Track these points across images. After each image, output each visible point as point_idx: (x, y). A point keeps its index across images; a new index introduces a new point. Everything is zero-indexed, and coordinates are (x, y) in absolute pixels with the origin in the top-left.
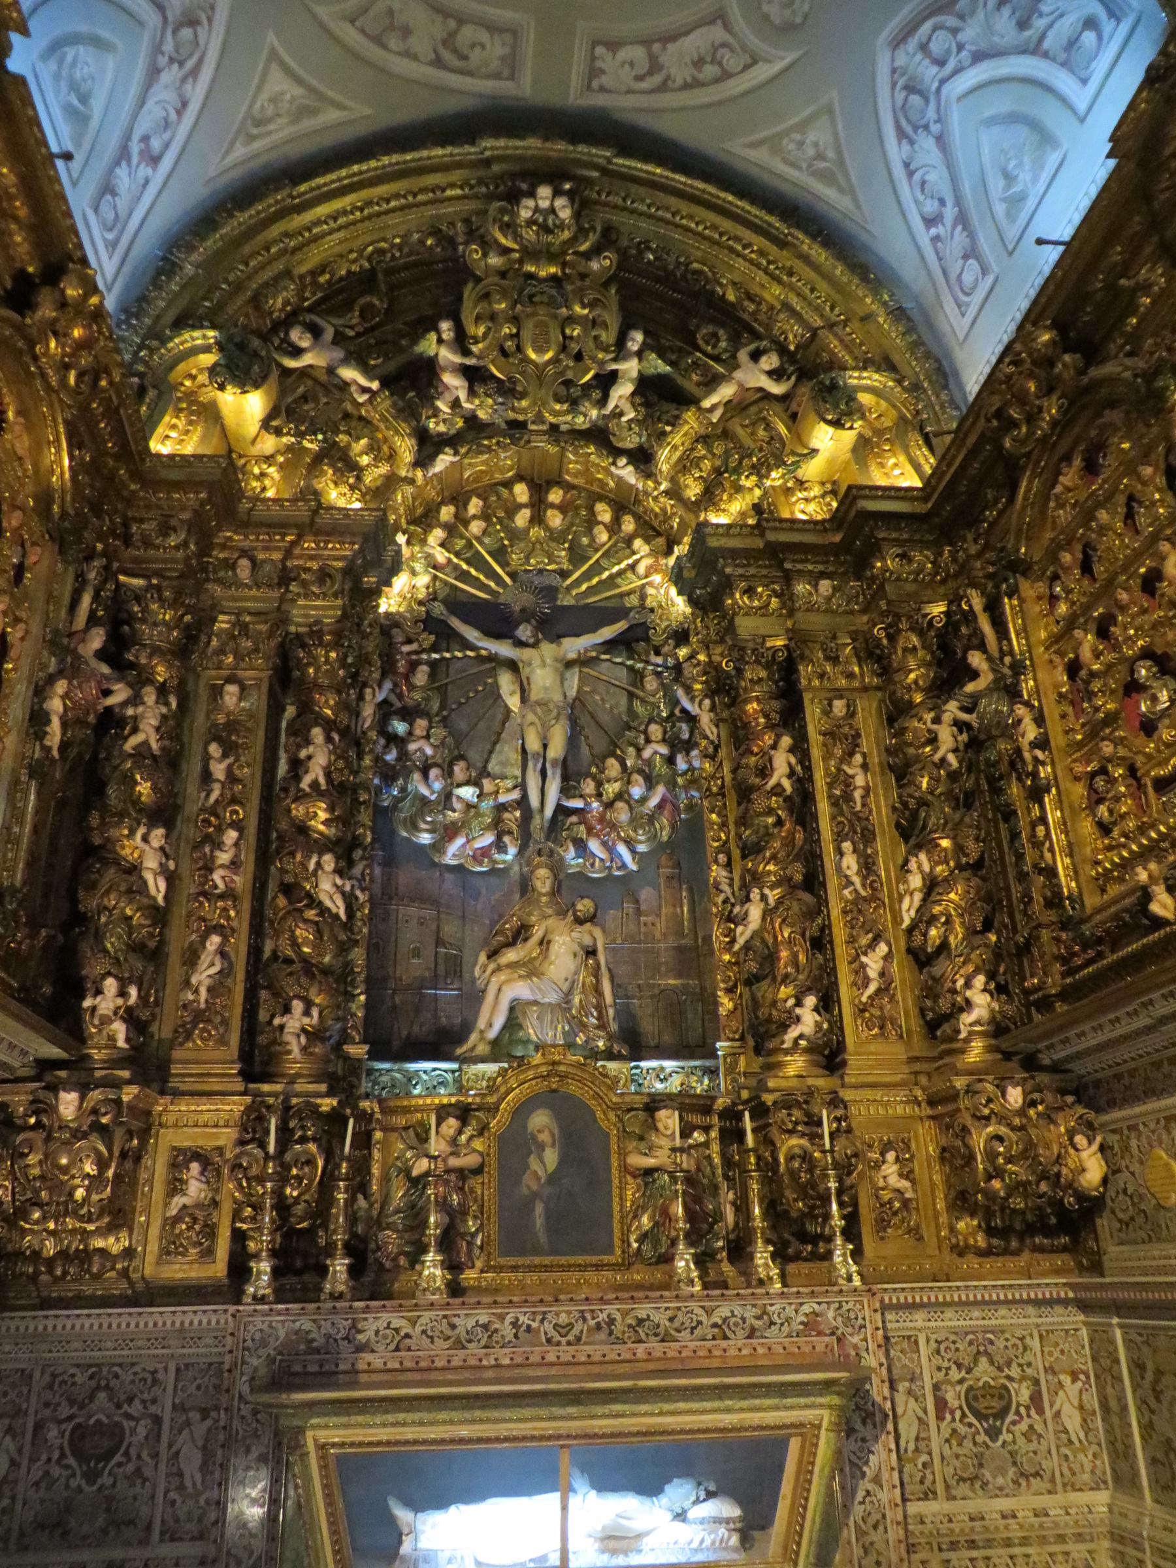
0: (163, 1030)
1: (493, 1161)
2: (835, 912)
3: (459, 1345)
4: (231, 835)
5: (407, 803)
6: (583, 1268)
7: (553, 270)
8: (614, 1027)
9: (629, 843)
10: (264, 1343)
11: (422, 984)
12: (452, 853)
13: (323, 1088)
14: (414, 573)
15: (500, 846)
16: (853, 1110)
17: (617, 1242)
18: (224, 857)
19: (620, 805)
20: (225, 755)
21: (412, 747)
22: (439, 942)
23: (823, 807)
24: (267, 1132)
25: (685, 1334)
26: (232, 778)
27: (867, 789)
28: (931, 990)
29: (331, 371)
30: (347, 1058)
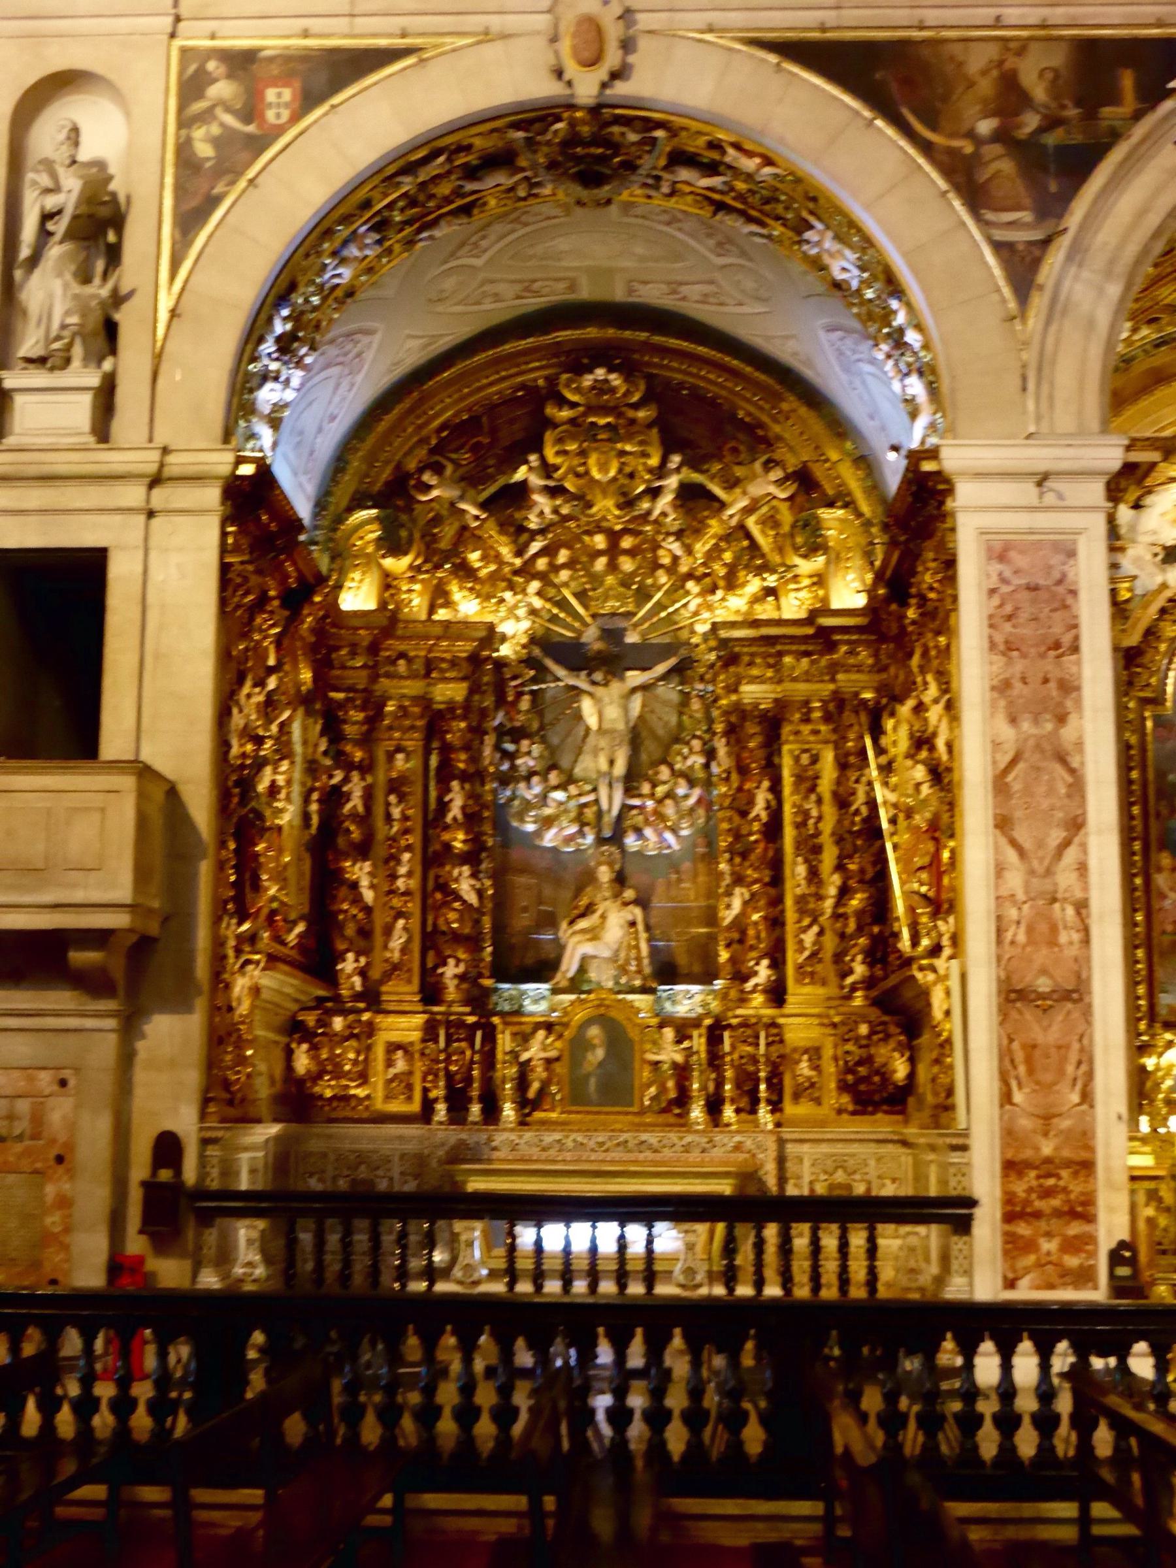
0: (375, 974)
2: (789, 902)
3: (544, 1149)
4: (406, 856)
5: (516, 803)
7: (609, 420)
9: (674, 830)
10: (443, 1144)
11: (528, 931)
12: (550, 839)
13: (467, 1009)
14: (518, 619)
15: (581, 833)
17: (636, 1101)
18: (403, 870)
19: (669, 802)
20: (400, 802)
21: (519, 762)
23: (789, 834)
24: (438, 1036)
25: (666, 1150)
26: (405, 818)
27: (820, 818)
29: (452, 504)
30: (481, 987)
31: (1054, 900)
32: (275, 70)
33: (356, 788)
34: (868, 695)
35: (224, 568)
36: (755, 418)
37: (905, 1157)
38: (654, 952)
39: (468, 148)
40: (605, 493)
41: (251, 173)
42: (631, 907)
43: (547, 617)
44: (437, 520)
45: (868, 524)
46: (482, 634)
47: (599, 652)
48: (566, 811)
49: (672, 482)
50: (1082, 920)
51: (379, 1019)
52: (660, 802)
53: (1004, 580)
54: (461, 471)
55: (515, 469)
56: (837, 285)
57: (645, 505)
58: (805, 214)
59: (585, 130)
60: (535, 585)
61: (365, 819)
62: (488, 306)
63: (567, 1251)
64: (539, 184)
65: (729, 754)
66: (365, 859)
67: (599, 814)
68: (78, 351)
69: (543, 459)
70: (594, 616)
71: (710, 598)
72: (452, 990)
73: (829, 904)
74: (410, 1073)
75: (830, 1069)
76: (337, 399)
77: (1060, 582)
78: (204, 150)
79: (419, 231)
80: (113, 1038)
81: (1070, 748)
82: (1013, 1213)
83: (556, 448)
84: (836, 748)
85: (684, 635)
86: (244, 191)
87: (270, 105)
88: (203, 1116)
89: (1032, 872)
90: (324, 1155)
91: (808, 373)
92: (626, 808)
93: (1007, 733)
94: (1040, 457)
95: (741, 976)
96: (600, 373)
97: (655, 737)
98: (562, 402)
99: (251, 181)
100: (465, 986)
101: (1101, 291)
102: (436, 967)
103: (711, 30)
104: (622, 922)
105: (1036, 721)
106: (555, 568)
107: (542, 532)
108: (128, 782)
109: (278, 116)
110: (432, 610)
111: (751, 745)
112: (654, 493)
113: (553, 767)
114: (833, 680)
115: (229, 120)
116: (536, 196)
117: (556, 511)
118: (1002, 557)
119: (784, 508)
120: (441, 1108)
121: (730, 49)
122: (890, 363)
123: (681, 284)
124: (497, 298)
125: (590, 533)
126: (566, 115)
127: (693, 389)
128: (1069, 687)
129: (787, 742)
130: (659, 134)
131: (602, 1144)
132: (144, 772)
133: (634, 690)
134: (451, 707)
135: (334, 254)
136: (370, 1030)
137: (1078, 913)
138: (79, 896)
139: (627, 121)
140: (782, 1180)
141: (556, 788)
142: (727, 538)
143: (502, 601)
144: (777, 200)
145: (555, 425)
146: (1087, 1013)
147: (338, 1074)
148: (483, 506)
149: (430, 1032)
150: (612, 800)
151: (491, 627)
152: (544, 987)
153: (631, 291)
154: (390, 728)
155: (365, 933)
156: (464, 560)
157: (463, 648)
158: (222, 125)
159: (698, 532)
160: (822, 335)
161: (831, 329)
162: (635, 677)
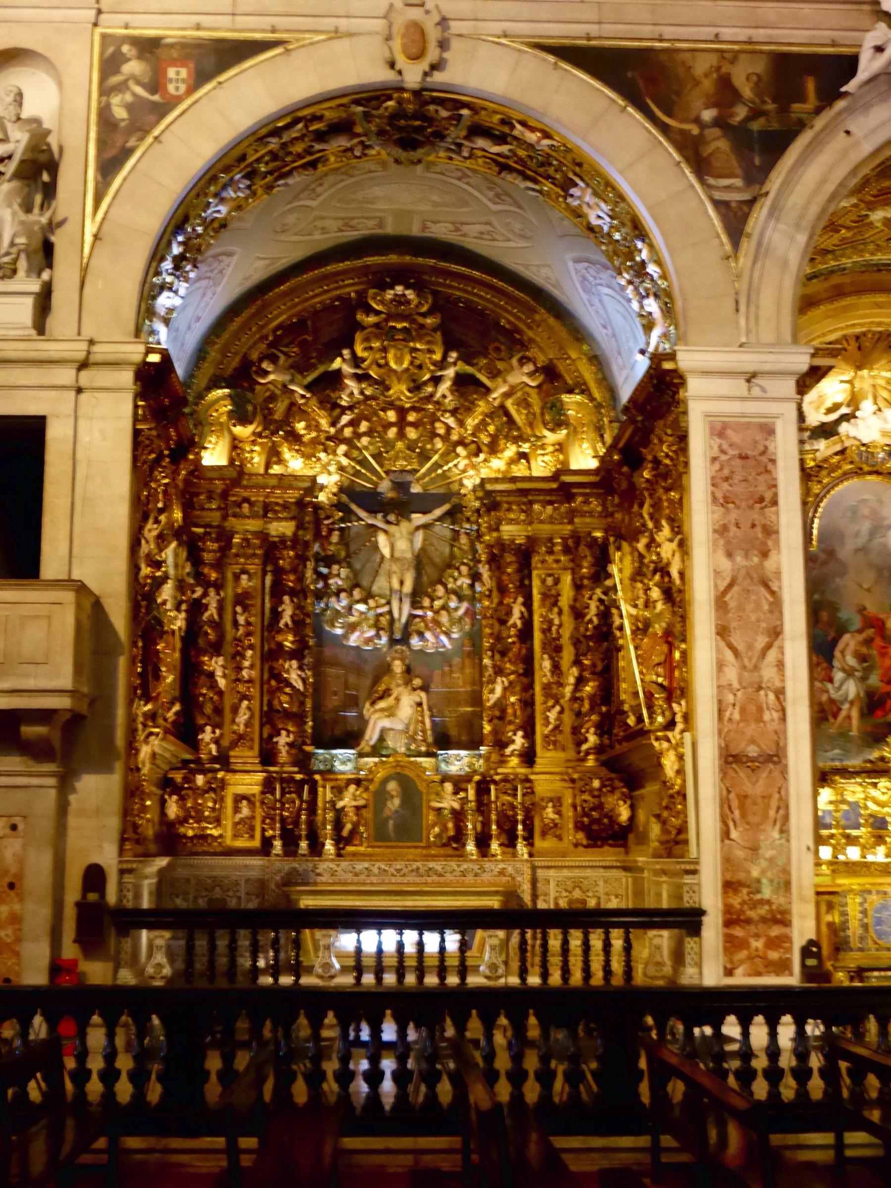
0: (225, 743)
1: (371, 803)
2: (538, 688)
3: (356, 875)
4: (249, 653)
6: (409, 847)
7: (405, 324)
8: (430, 739)
9: (447, 634)
10: (279, 871)
11: (337, 710)
12: (354, 640)
13: (296, 769)
14: (330, 473)
15: (378, 636)
16: (536, 784)
18: (246, 664)
21: (331, 581)
22: (347, 687)
23: (538, 636)
24: (275, 789)
26: (248, 624)
27: (560, 626)
28: (575, 730)
31: (760, 688)
32: (175, 54)
33: (212, 601)
34: (598, 534)
35: (136, 433)
36: (514, 325)
37: (625, 879)
38: (434, 724)
39: (320, 118)
40: (399, 380)
41: (156, 132)
42: (418, 692)
43: (351, 471)
44: (272, 398)
45: (599, 406)
46: (307, 484)
47: (392, 499)
48: (367, 619)
49: (450, 372)
50: (781, 703)
51: (229, 776)
52: (437, 612)
53: (723, 452)
54: (291, 361)
55: (332, 361)
56: (591, 229)
57: (430, 389)
58: (571, 175)
59: (410, 107)
60: (343, 448)
61: (218, 626)
62: (317, 236)
63: (380, 951)
64: (369, 147)
65: (491, 578)
66: (219, 655)
67: (392, 621)
68: (22, 264)
69: (353, 353)
70: (387, 472)
71: (474, 459)
72: (284, 755)
73: (568, 690)
74: (253, 818)
75: (569, 813)
76: (203, 304)
77: (763, 453)
78: (120, 113)
79: (277, 179)
80: (53, 793)
81: (771, 576)
82: (731, 919)
83: (366, 345)
84: (574, 573)
85: (455, 487)
86: (151, 145)
87: (171, 80)
88: (121, 851)
89: (744, 667)
90: (188, 881)
91: (556, 292)
92: (412, 617)
93: (725, 564)
94: (749, 361)
95: (501, 744)
96: (399, 289)
97: (434, 564)
98: (369, 310)
99: (156, 138)
100: (293, 751)
101: (792, 239)
102: (271, 737)
103: (505, 36)
104: (412, 703)
105: (746, 556)
106: (358, 436)
107: (351, 408)
108: (69, 597)
109: (177, 88)
110: (268, 466)
111: (509, 570)
112: (436, 380)
113: (357, 585)
114: (571, 522)
115: (139, 90)
116: (365, 155)
117: (362, 393)
118: (721, 434)
119: (534, 393)
120: (278, 844)
121: (520, 50)
122: (631, 287)
123: (462, 224)
124: (324, 230)
125: (384, 410)
126: (395, 95)
127: (467, 302)
128: (771, 531)
129: (537, 568)
130: (465, 112)
131: (398, 871)
132: (81, 589)
133: (418, 528)
134: (283, 539)
135: (216, 195)
136: (223, 784)
137: (778, 698)
138: (31, 684)
139: (442, 102)
140: (535, 896)
141: (358, 602)
142: (491, 415)
143: (319, 459)
144: (550, 164)
145: (363, 328)
146: (784, 772)
147: (200, 819)
148: (307, 388)
149: (268, 786)
150: (402, 611)
151: (313, 479)
152: (349, 753)
153: (424, 228)
154: (237, 555)
155: (218, 711)
156: (293, 428)
157: (292, 496)
158: (134, 95)
159: (469, 410)
160: (570, 264)
161: (577, 261)
162: (418, 519)
